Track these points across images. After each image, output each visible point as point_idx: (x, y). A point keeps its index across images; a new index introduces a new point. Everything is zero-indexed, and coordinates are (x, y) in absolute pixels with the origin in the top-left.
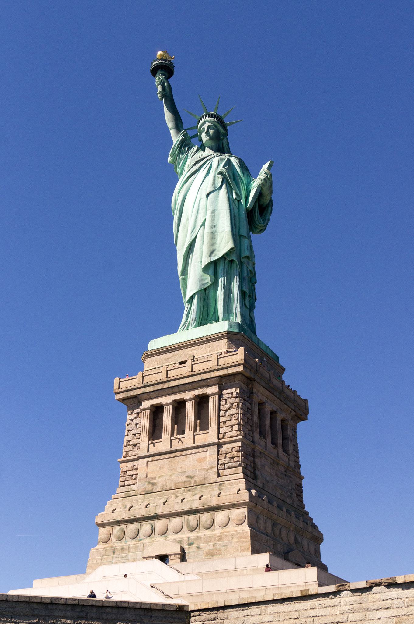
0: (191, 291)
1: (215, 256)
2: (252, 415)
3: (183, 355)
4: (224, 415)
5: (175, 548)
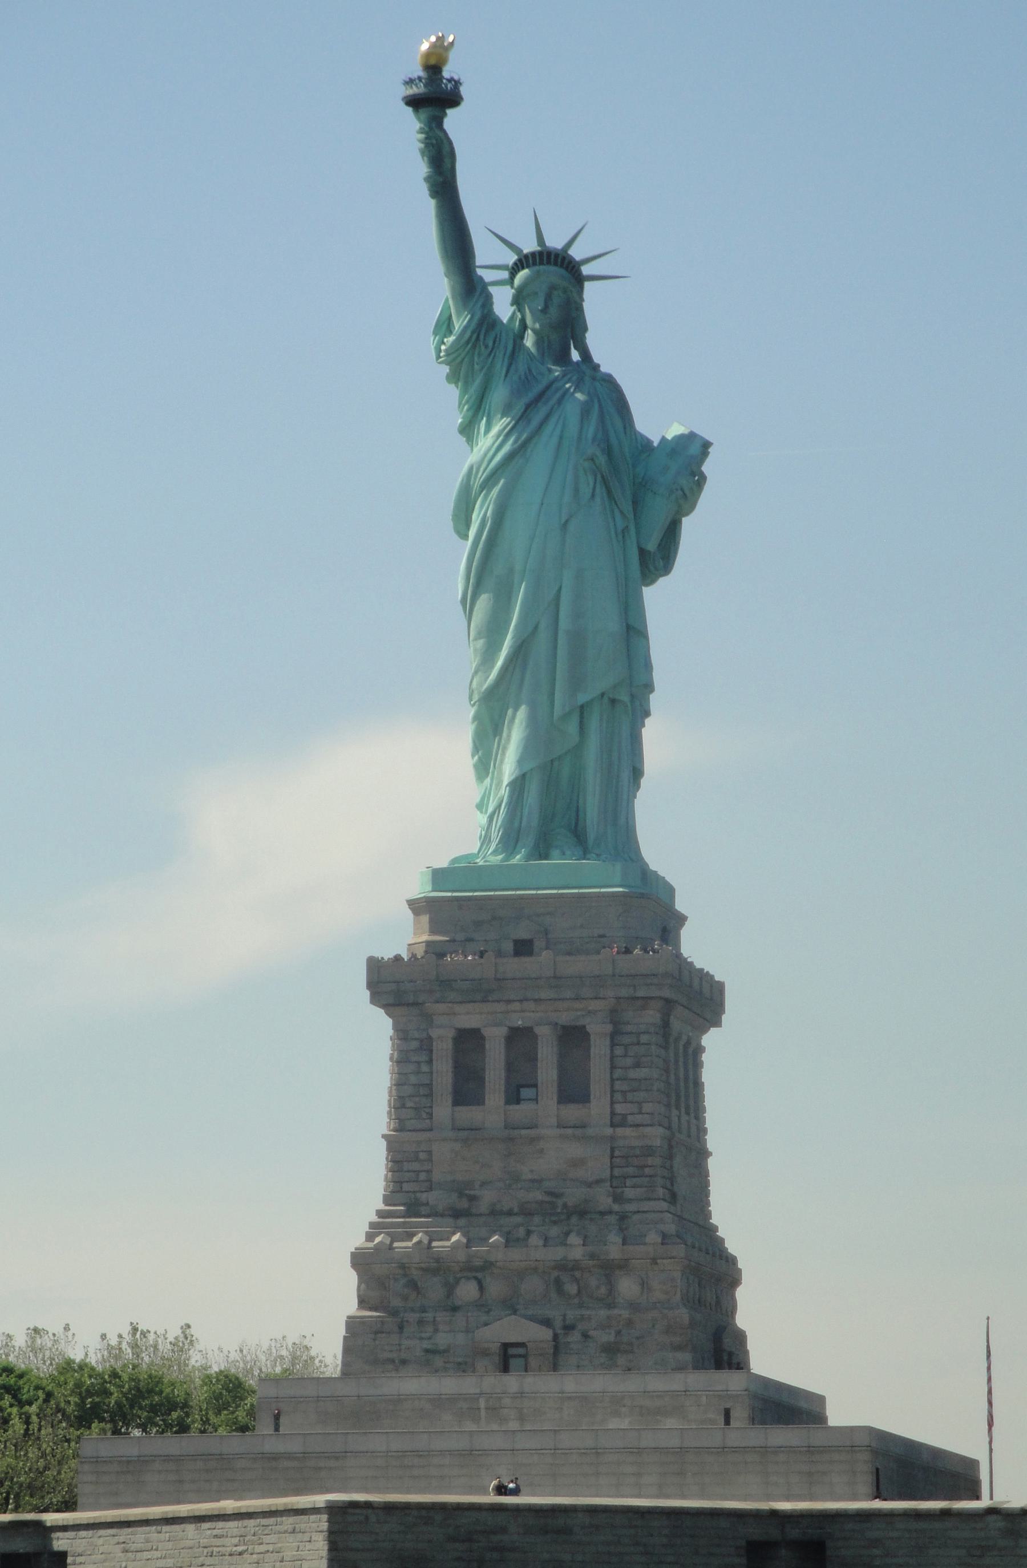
2: (667, 1071)
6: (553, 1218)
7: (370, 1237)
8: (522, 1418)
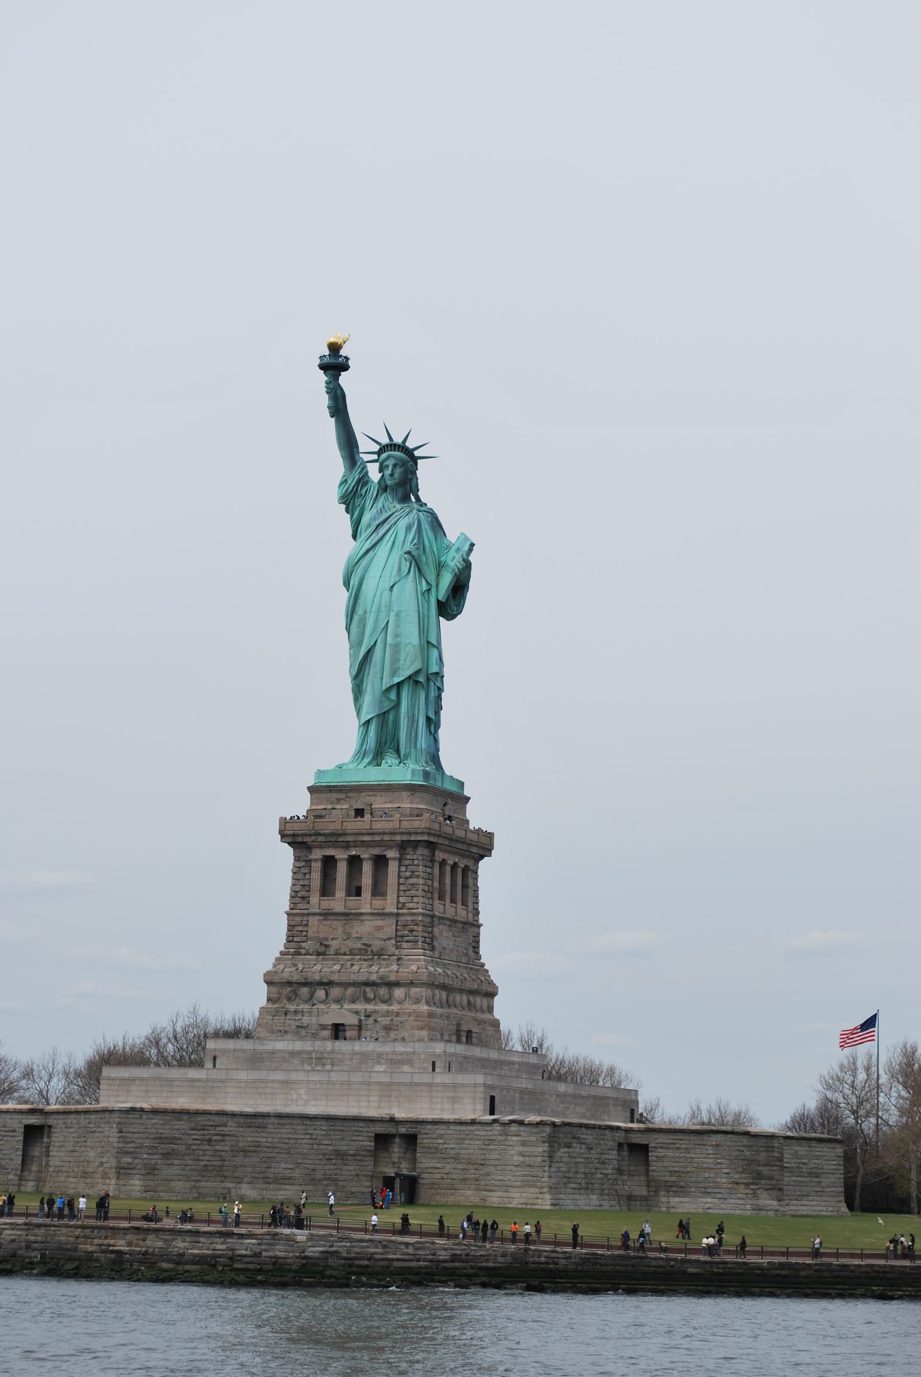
0: (368, 713)
2: (432, 880)
3: (359, 802)
6: (366, 957)
7: (275, 966)
8: (332, 1064)
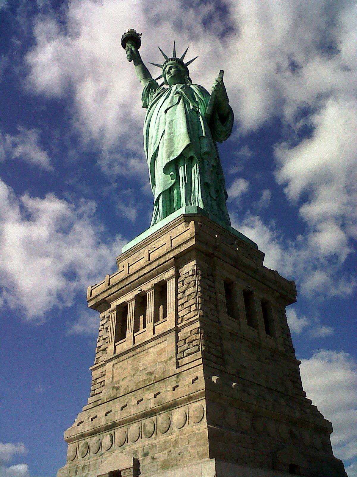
1: (173, 156)
4: (181, 297)
5: (127, 461)
